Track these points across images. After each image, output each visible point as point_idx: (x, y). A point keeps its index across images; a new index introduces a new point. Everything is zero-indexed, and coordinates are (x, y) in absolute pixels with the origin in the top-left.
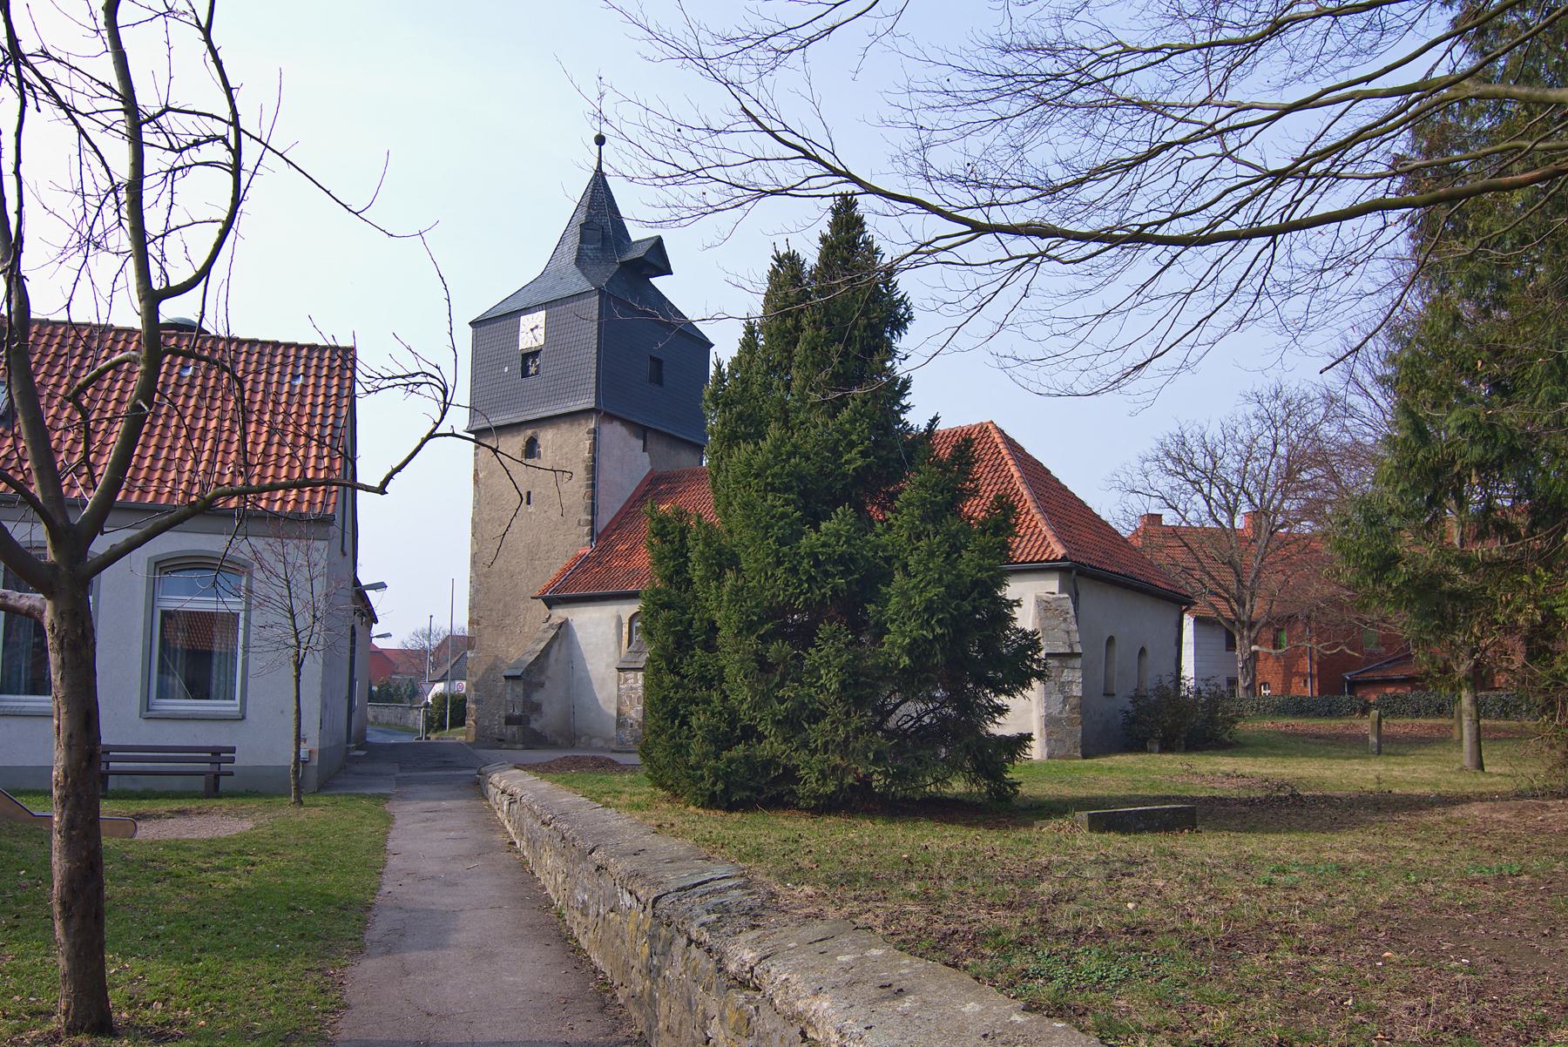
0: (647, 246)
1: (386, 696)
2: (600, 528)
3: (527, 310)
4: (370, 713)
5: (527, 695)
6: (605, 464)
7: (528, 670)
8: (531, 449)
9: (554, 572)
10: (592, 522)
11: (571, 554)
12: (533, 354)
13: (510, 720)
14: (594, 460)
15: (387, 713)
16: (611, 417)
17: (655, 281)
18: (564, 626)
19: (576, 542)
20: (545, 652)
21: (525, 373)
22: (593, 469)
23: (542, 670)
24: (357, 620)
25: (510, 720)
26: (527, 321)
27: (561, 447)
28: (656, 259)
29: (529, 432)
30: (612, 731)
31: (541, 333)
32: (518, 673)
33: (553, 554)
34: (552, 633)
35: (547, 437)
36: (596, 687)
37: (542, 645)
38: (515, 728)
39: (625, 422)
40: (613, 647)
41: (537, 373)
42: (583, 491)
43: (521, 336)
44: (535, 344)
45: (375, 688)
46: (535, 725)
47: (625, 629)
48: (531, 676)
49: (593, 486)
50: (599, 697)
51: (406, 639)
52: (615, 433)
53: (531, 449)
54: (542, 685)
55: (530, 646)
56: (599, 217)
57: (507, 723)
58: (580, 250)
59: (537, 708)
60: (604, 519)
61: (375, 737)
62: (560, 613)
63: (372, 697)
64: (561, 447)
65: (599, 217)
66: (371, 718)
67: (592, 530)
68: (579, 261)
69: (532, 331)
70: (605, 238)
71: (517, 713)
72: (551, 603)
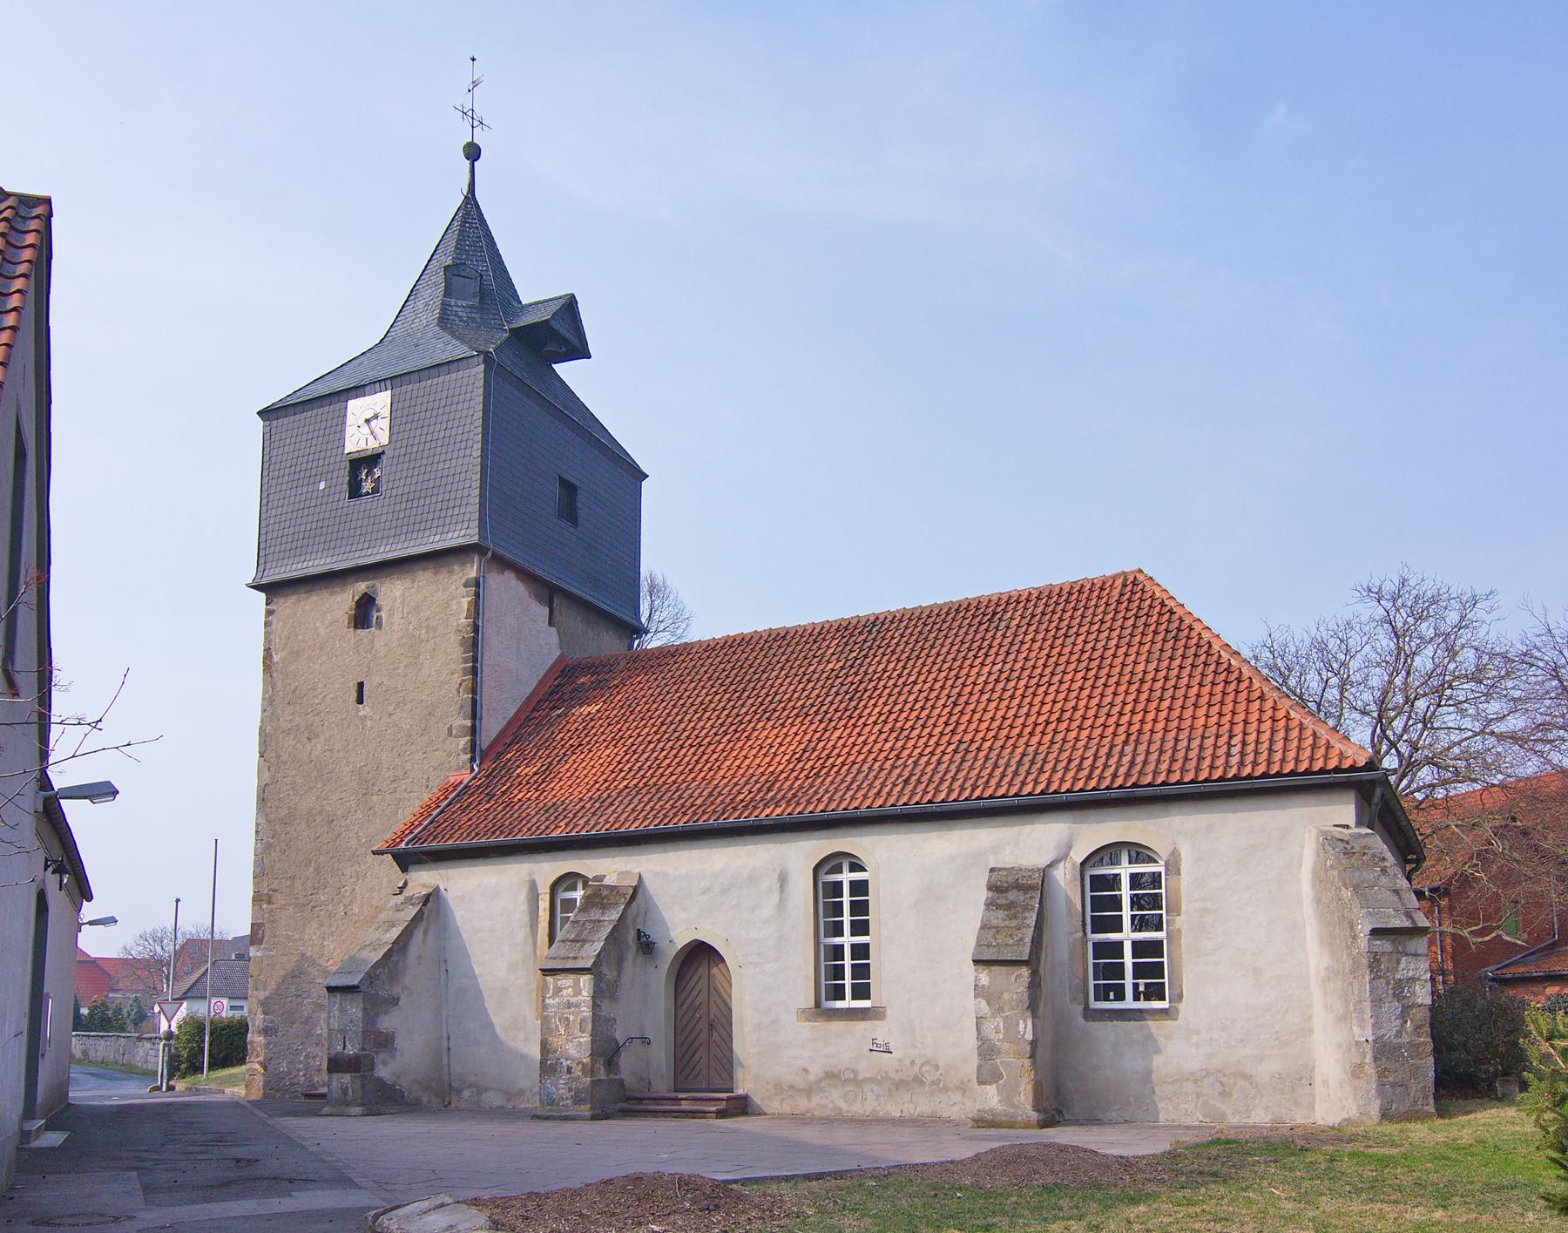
0: (555, 307)
1: (102, 1022)
2: (485, 740)
3: (358, 390)
4: (77, 1046)
5: (370, 1018)
6: (490, 634)
7: (371, 976)
8: (364, 613)
9: (405, 815)
10: (473, 730)
11: (437, 782)
12: (369, 461)
13: (336, 1065)
14: (476, 629)
15: (103, 1047)
16: (501, 562)
17: (564, 370)
18: (432, 899)
19: (445, 762)
20: (401, 945)
21: (355, 491)
22: (474, 645)
23: (394, 977)
24: (52, 880)
25: (336, 1065)
26: (357, 408)
27: (417, 609)
28: (561, 332)
29: (362, 587)
30: (528, 1079)
31: (383, 425)
32: (354, 980)
33: (403, 784)
34: (411, 912)
35: (392, 594)
36: (490, 1004)
37: (395, 933)
38: (347, 1078)
39: (523, 574)
40: (522, 934)
41: (375, 490)
42: (457, 679)
43: (349, 431)
44: (373, 445)
45: (85, 1011)
46: (383, 1072)
47: (544, 904)
48: (372, 989)
49: (474, 671)
50: (496, 1020)
51: (130, 943)
52: (507, 590)
53: (364, 613)
54: (394, 1001)
55: (372, 934)
56: (469, 259)
57: (330, 1070)
58: (444, 307)
59: (385, 1042)
60: (492, 727)
61: (87, 1092)
62: (423, 879)
63: (79, 1023)
64: (417, 609)
65: (469, 259)
66: (78, 1055)
67: (473, 743)
68: (444, 321)
69: (366, 423)
70: (483, 294)
71: (351, 1050)
72: (405, 861)
